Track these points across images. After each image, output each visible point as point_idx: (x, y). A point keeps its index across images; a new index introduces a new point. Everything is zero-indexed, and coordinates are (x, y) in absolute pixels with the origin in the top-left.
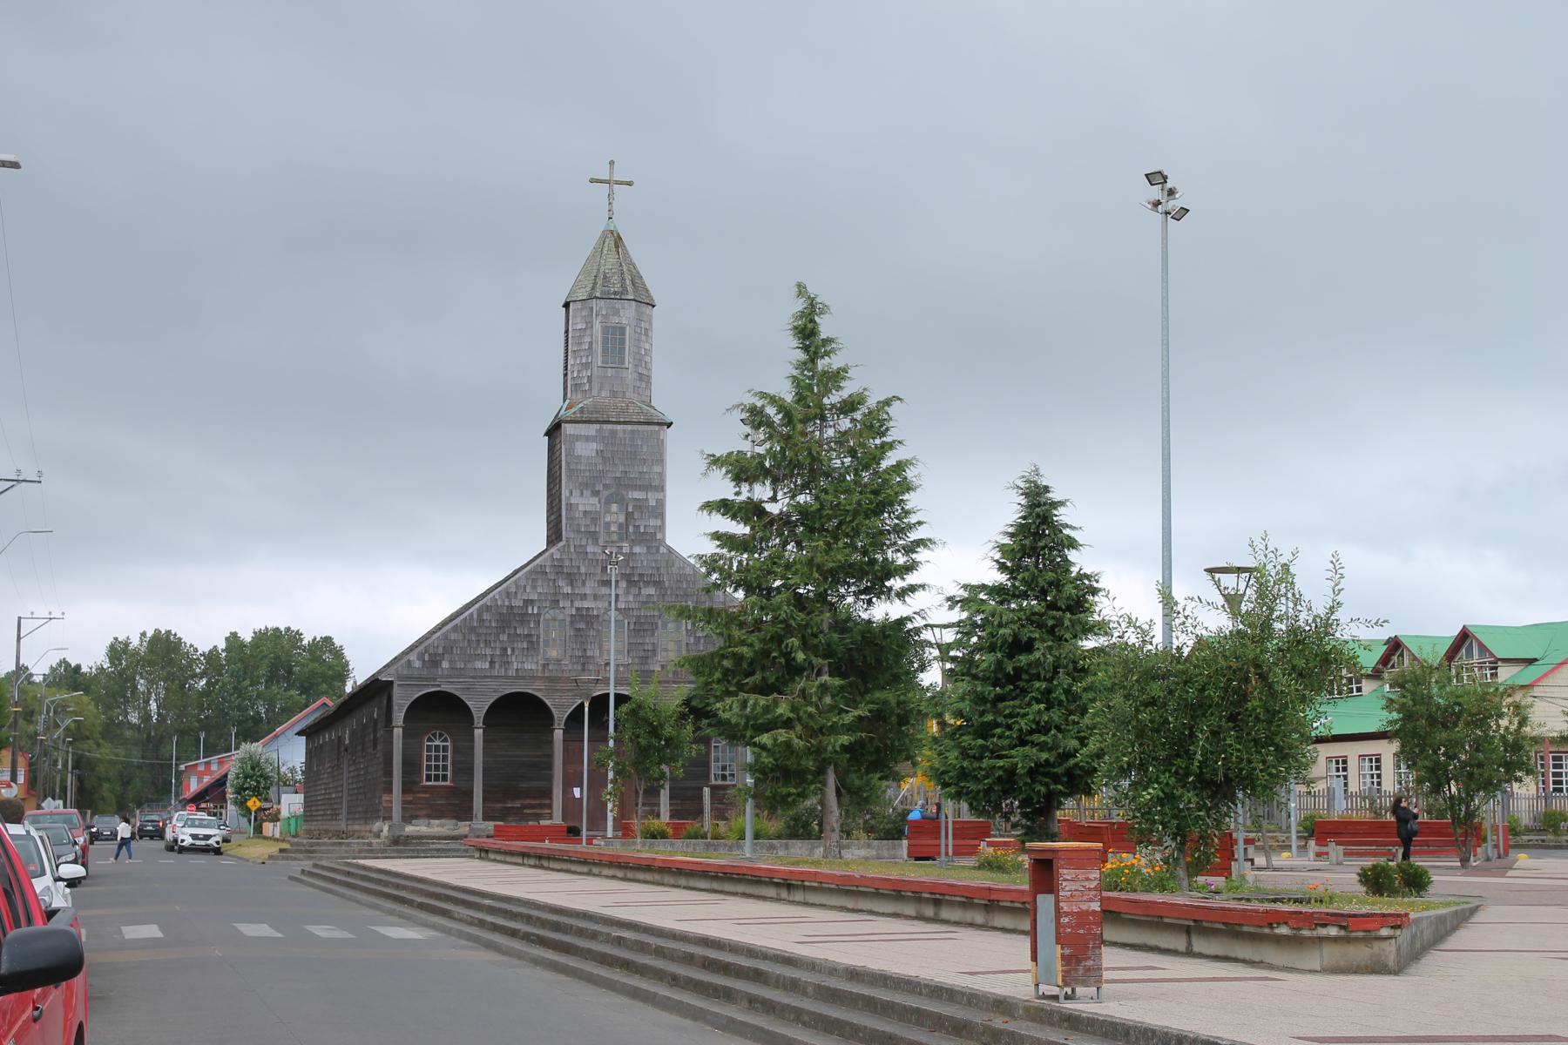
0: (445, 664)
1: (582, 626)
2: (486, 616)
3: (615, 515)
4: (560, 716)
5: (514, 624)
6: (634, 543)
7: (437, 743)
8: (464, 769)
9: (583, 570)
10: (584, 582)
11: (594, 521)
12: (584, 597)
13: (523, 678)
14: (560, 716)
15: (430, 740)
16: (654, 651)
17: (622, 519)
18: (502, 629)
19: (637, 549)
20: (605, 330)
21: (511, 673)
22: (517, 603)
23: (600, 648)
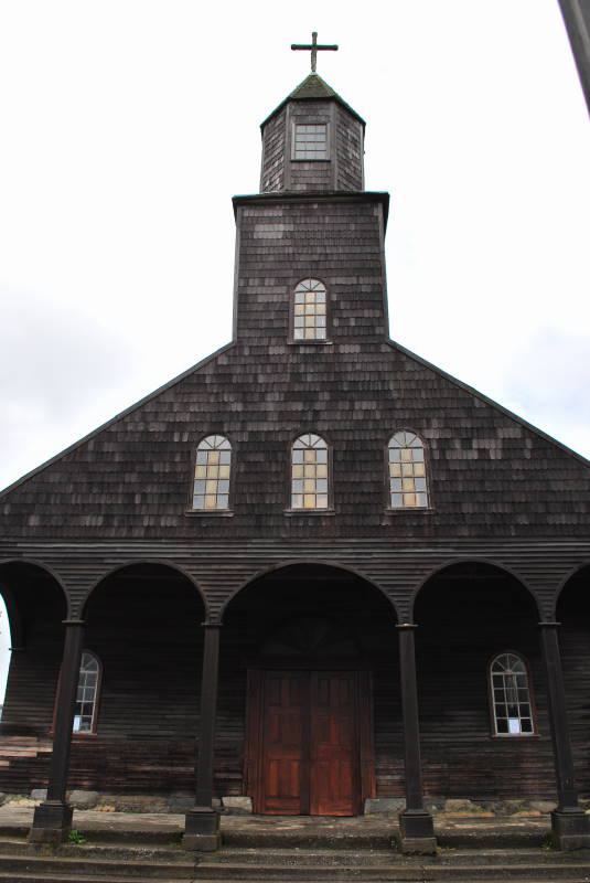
0: (34, 521)
1: (260, 458)
4: (215, 608)
9: (261, 379)
10: (263, 400)
12: (263, 416)
14: (215, 608)
18: (126, 467)
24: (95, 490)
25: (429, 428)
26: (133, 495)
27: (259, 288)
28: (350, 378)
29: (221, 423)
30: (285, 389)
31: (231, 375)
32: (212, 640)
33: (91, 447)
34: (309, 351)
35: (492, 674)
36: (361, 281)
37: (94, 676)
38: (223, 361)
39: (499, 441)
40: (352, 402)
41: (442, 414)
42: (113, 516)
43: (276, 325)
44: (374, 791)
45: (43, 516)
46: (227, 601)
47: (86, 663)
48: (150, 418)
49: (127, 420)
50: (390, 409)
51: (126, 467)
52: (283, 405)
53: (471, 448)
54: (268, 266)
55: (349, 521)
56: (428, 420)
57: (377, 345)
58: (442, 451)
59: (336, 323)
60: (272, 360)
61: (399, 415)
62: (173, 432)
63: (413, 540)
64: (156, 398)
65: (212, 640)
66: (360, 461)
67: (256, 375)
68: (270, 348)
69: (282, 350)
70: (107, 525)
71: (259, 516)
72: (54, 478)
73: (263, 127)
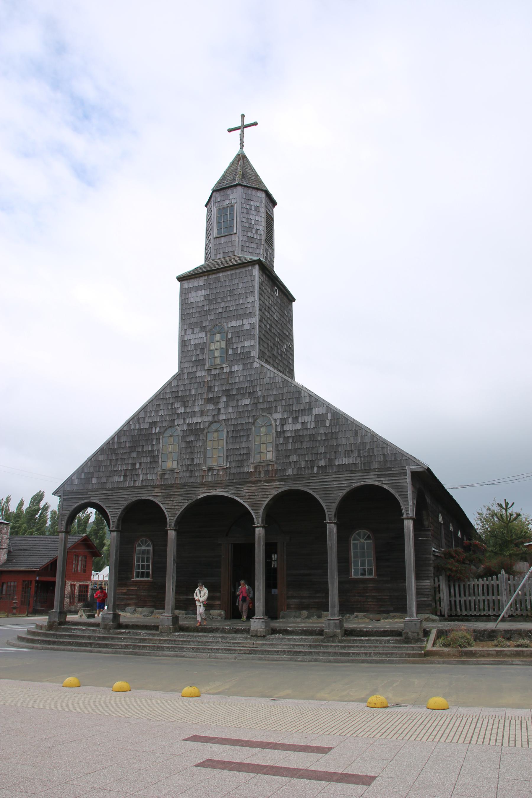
0: (94, 481)
1: (191, 438)
2: (123, 439)
3: (218, 344)
4: (171, 519)
5: (143, 443)
6: (231, 364)
7: (143, 548)
8: (160, 569)
9: (193, 392)
10: (194, 405)
11: (203, 350)
12: (193, 414)
13: (146, 487)
14: (171, 519)
15: (140, 546)
16: (248, 454)
17: (223, 344)
19: (235, 368)
20: (219, 210)
21: (138, 483)
22: (145, 426)
23: (205, 457)
24: (119, 463)
25: (276, 412)
26: (135, 464)
27: (192, 336)
28: (237, 386)
29: (174, 420)
30: (205, 396)
31: (178, 391)
32: (172, 534)
33: (116, 440)
34: (217, 372)
35: (352, 542)
36: (245, 321)
37: (148, 550)
38: (174, 384)
39: (313, 417)
40: (237, 400)
41: (283, 402)
42: (127, 476)
43: (200, 357)
44: (286, 608)
45: (98, 478)
46: (177, 516)
47: (146, 543)
48: (141, 421)
49: (131, 423)
50: (256, 403)
51: (132, 449)
52: (203, 406)
53: (298, 422)
54: (196, 320)
55: (233, 471)
56: (276, 407)
57: (252, 364)
58: (282, 425)
59: (230, 352)
60: (198, 380)
61: (260, 406)
62: (152, 428)
63: (264, 479)
64: (144, 408)
65: (172, 534)
66: (240, 436)
67: (190, 390)
68: (197, 373)
69: (203, 373)
70: (125, 481)
71: (191, 471)
72: (101, 458)
73: (206, 206)
